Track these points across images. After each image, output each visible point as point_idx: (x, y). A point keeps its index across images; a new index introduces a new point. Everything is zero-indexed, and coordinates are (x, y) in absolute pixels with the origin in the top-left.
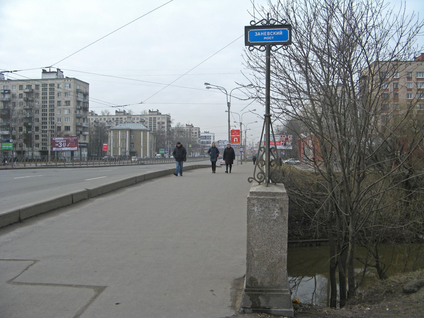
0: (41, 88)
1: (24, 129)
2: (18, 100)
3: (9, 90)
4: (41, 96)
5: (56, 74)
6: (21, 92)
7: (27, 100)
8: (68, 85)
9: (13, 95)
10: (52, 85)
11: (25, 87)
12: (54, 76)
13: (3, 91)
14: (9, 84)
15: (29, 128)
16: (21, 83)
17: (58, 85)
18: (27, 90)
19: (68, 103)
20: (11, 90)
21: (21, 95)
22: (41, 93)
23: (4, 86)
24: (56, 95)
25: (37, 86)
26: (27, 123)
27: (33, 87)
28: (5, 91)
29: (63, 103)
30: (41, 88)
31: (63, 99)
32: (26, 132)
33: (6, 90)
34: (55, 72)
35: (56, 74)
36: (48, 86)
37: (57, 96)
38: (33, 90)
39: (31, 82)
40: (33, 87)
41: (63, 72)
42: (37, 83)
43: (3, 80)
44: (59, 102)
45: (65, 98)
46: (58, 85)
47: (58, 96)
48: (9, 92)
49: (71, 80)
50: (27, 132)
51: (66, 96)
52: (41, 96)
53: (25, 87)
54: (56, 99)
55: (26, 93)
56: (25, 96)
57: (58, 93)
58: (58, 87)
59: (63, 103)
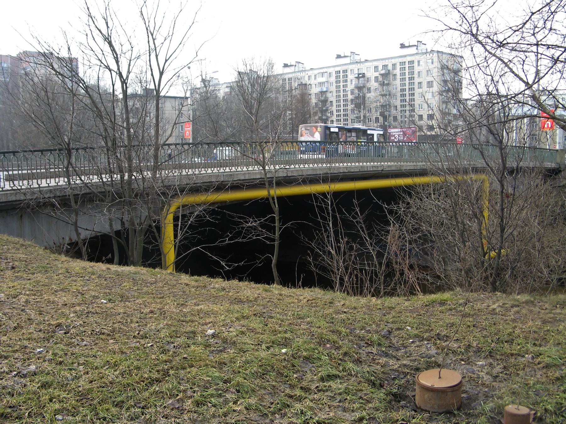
0: (398, 67)
1: (381, 119)
2: (373, 85)
3: (364, 74)
4: (398, 77)
5: (416, 47)
6: (377, 74)
7: (383, 84)
8: (430, 61)
9: (368, 78)
10: (412, 62)
11: (380, 68)
12: (413, 50)
13: (357, 76)
14: (364, 65)
15: (385, 118)
16: (376, 64)
17: (419, 62)
18: (383, 72)
19: (430, 84)
20: (366, 73)
21: (376, 78)
22: (398, 74)
23: (358, 69)
24: (416, 75)
25: (394, 65)
26: (384, 112)
27: (390, 67)
28: (359, 74)
29: (425, 85)
30: (398, 67)
31: (425, 79)
32: (382, 124)
33: (360, 74)
34: (415, 46)
35: (416, 47)
36: (407, 63)
37: (417, 76)
38: (389, 71)
39: (387, 61)
40: (390, 67)
41: (425, 44)
42: (394, 61)
43: (358, 61)
44: (420, 83)
45: (427, 78)
46: (419, 62)
47: (419, 76)
48: (364, 75)
49: (434, 54)
50: (384, 123)
51: (428, 75)
52: (398, 77)
53: (380, 68)
54: (417, 80)
55: (382, 75)
56: (380, 79)
57: (419, 72)
58: (419, 65)
59: (425, 85)
